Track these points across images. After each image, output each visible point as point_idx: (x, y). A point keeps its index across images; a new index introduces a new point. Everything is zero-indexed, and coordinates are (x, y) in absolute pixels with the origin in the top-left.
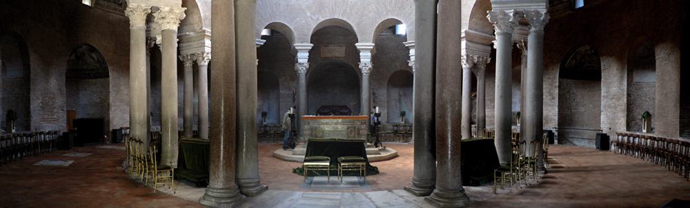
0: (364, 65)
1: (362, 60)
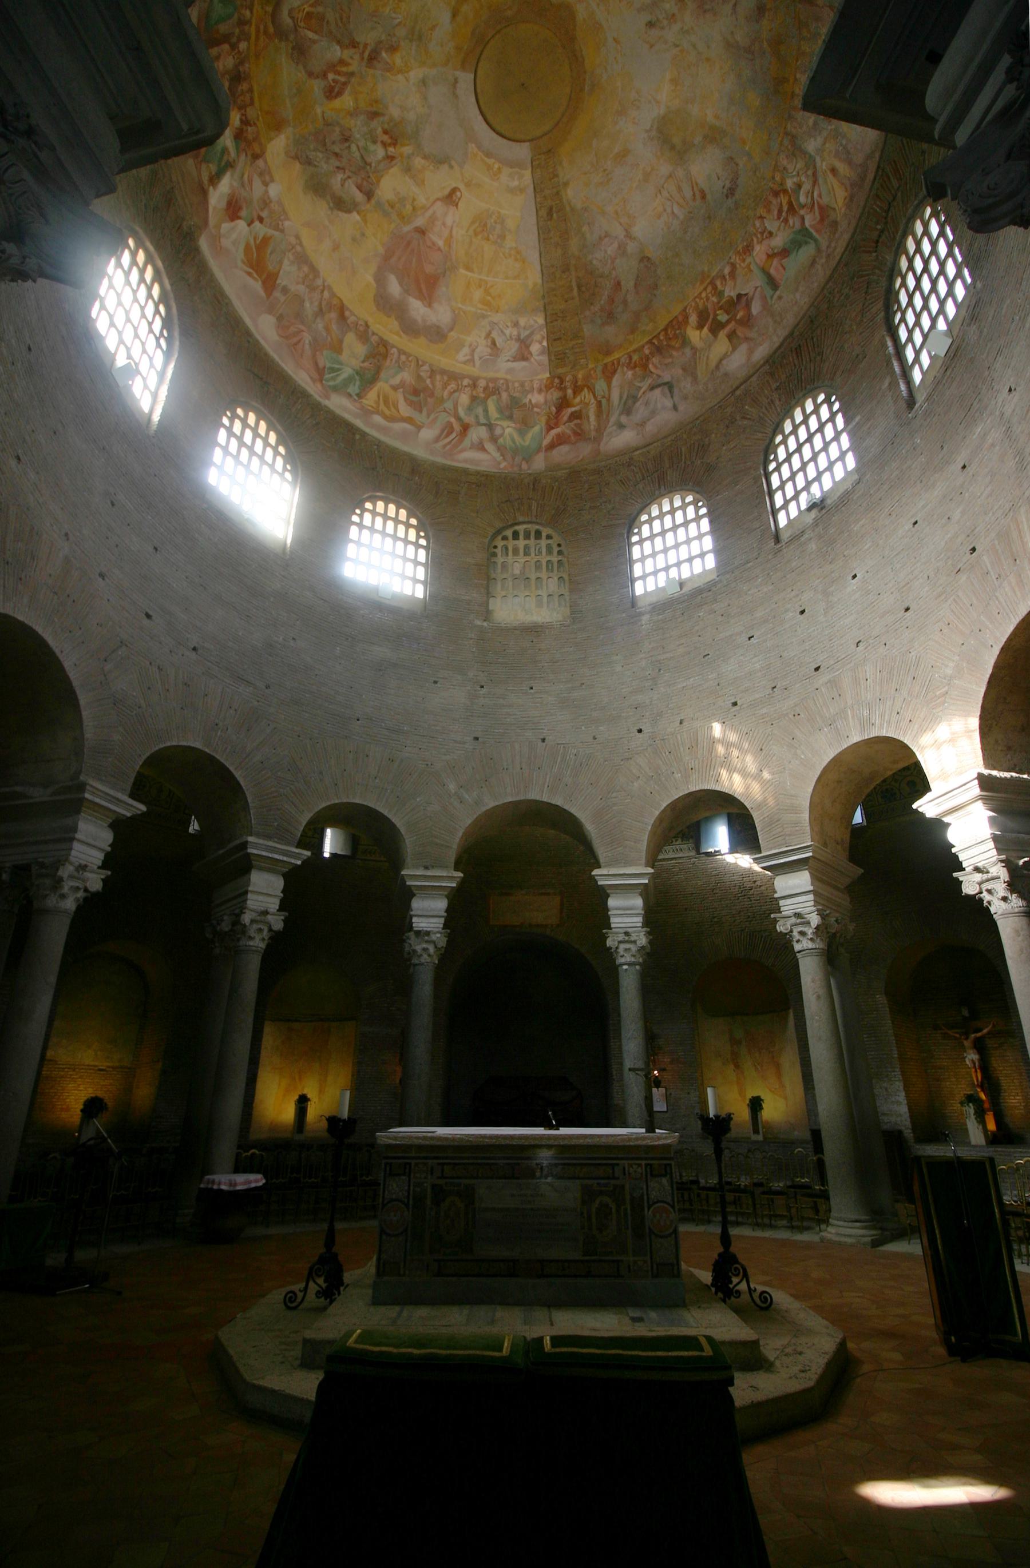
0: (621, 937)
1: (615, 921)
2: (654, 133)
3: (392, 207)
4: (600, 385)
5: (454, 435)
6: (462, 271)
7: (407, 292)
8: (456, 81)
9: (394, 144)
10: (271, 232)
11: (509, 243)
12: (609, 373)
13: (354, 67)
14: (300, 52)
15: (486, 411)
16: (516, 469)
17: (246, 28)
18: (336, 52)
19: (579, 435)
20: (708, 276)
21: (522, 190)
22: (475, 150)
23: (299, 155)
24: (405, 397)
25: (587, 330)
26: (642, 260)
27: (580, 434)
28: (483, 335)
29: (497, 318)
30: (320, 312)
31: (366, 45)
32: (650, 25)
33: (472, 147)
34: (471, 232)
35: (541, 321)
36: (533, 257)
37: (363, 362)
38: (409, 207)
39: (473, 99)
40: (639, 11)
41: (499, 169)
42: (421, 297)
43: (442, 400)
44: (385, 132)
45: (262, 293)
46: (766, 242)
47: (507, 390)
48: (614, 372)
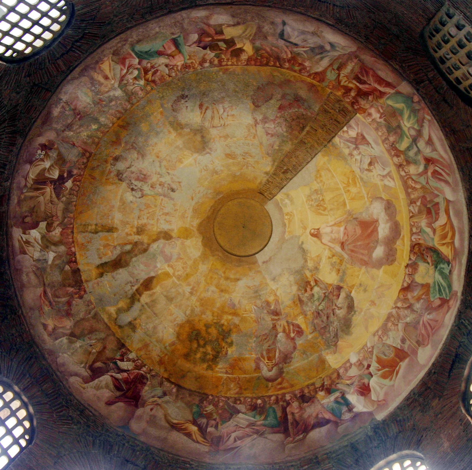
2: (208, 150)
3: (339, 270)
4: (331, 76)
5: (437, 169)
6: (348, 207)
7: (377, 242)
8: (264, 262)
9: (308, 282)
10: (374, 358)
11: (316, 186)
12: (321, 76)
13: (283, 322)
14: (286, 358)
15: (408, 149)
16: (423, 104)
17: (280, 397)
18: (281, 336)
19: (365, 70)
20: (221, 69)
21: (288, 195)
22: (287, 234)
23: (333, 344)
24: (435, 221)
25: (316, 108)
26: (258, 106)
27: (364, 69)
28: (372, 174)
29: (357, 171)
30: (410, 307)
31: (273, 320)
32: (173, 190)
33: (287, 236)
34: (326, 213)
35: (337, 140)
36: (311, 166)
37: (428, 263)
38: (334, 259)
39: (266, 248)
40: (173, 199)
41: (287, 215)
42: (375, 230)
43: (423, 187)
44: (306, 291)
45: (407, 360)
46: (171, 63)
47: (387, 139)
48: (316, 73)
